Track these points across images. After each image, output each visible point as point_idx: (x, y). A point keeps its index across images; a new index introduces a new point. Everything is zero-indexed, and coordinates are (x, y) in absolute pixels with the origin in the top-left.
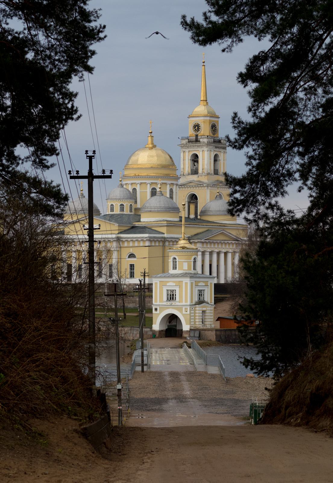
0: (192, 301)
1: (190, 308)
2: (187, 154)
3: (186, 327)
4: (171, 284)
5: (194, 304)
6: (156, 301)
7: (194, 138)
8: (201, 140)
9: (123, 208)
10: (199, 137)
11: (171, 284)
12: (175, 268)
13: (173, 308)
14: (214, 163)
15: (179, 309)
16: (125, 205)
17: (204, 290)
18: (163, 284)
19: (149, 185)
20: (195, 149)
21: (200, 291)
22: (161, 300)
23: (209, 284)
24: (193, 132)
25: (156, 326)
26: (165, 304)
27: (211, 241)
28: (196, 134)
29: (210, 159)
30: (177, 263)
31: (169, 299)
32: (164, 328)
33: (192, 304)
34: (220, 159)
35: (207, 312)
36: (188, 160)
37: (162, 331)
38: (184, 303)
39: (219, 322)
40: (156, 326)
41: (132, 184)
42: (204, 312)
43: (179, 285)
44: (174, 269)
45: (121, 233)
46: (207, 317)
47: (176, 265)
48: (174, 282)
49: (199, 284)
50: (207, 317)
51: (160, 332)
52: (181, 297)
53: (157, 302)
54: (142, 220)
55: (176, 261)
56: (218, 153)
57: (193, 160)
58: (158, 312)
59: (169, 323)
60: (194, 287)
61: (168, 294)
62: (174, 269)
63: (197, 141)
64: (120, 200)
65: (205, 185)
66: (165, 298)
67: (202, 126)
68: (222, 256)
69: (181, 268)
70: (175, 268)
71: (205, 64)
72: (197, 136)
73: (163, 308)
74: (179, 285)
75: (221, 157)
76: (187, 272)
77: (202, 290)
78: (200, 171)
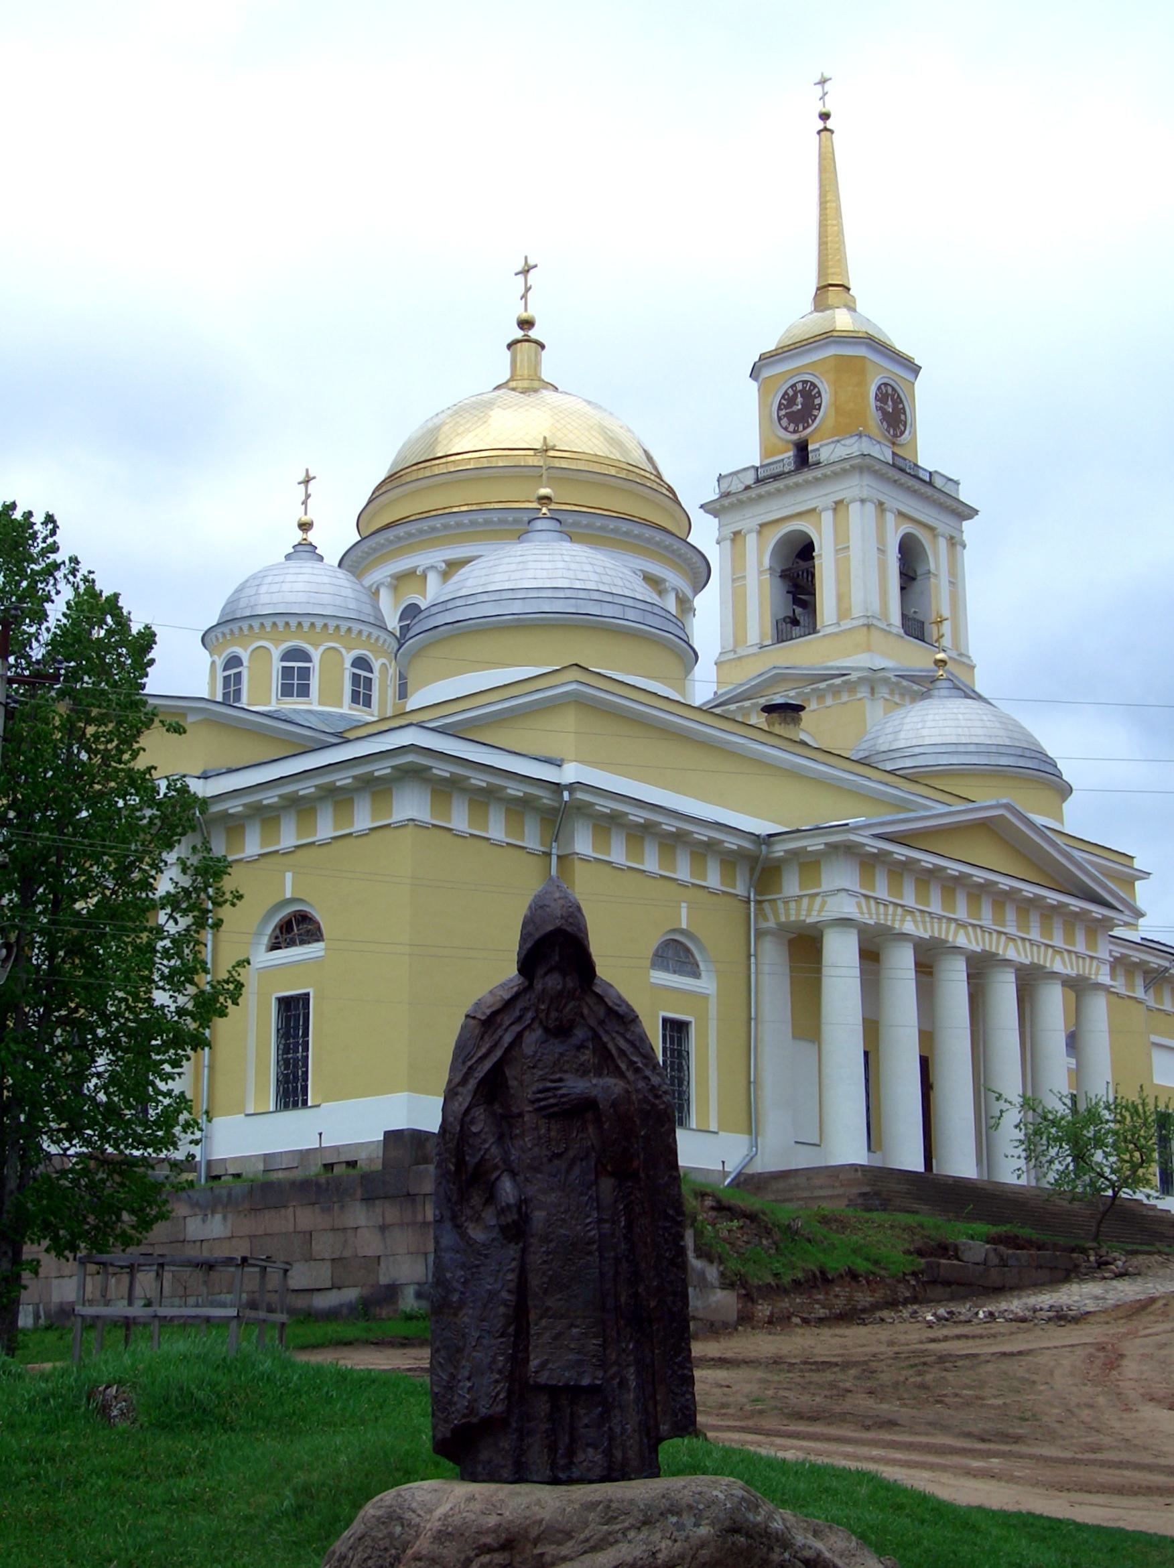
2: (751, 540)
9: (305, 673)
14: (902, 588)
16: (316, 654)
24: (782, 433)
27: (928, 860)
28: (795, 437)
29: (882, 551)
34: (932, 567)
36: (761, 573)
56: (923, 536)
57: (785, 575)
64: (280, 622)
65: (854, 676)
68: (1005, 991)
71: (830, 124)
72: (802, 449)
75: (937, 557)
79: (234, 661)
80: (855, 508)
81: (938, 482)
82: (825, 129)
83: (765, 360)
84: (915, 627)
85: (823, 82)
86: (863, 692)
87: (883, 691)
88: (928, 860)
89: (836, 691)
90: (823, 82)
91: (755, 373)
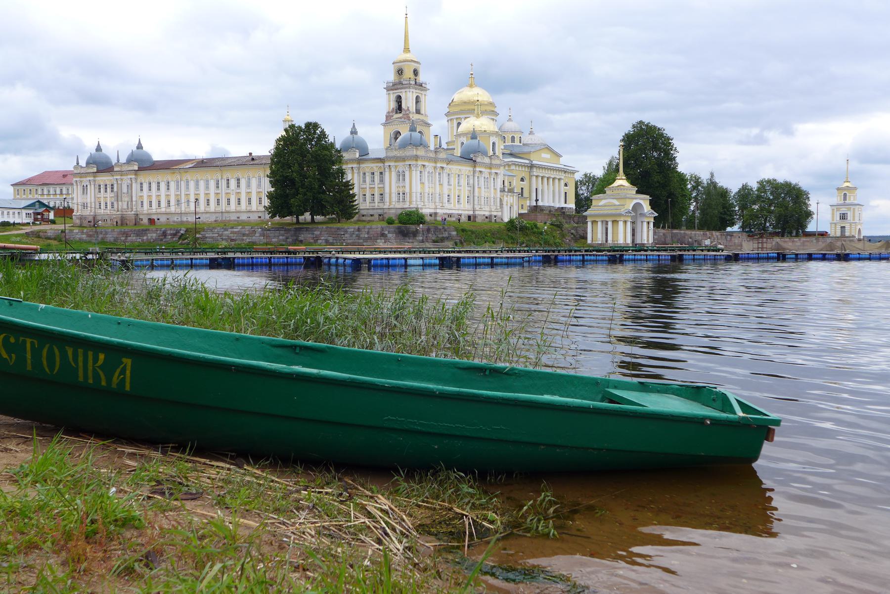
20: (419, 91)
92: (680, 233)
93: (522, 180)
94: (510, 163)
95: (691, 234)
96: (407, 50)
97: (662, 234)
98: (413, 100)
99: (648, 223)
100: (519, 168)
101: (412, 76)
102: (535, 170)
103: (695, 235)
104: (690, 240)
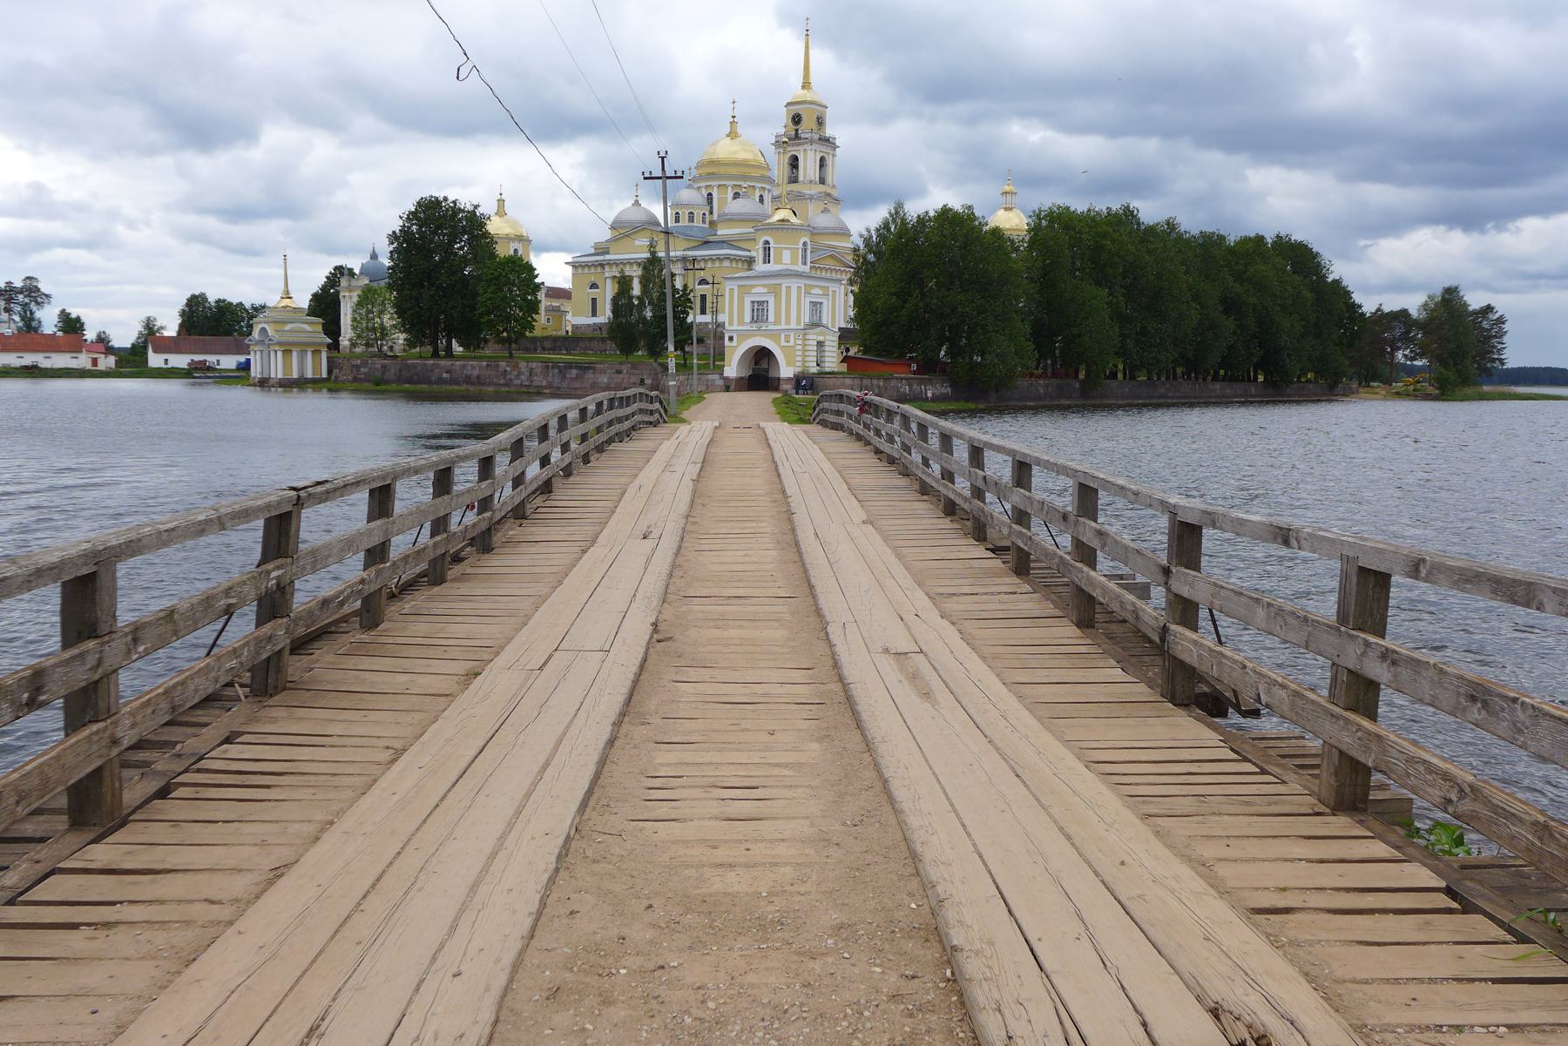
0: (798, 322)
1: (795, 334)
3: (786, 371)
4: (759, 291)
5: (802, 327)
6: (731, 323)
7: (794, 133)
8: (802, 136)
10: (799, 132)
11: (759, 291)
12: (767, 260)
13: (762, 335)
15: (775, 335)
17: (821, 303)
18: (744, 291)
19: (730, 188)
20: (794, 148)
21: (814, 304)
22: (741, 322)
23: (830, 293)
25: (732, 370)
26: (748, 328)
27: (817, 265)
29: (815, 162)
30: (771, 249)
31: (755, 318)
32: (746, 373)
33: (798, 327)
35: (827, 343)
37: (741, 378)
38: (783, 326)
39: (845, 365)
40: (732, 370)
41: (707, 187)
42: (820, 344)
43: (775, 291)
44: (765, 262)
45: (688, 249)
46: (826, 354)
47: (769, 254)
48: (764, 286)
49: (812, 292)
50: (826, 354)
51: (739, 380)
52: (777, 314)
53: (733, 325)
54: (718, 233)
55: (769, 248)
58: (735, 343)
59: (755, 365)
60: (803, 298)
61: (753, 310)
62: (765, 262)
63: (797, 136)
66: (748, 318)
67: (804, 117)
69: (779, 261)
70: (767, 260)
72: (797, 130)
73: (744, 335)
74: (775, 291)
75: (829, 161)
76: (791, 267)
77: (817, 303)
78: (801, 178)
79: (677, 213)
80: (809, 152)
81: (831, 140)
82: (807, 35)
83: (789, 104)
84: (822, 181)
85: (807, 19)
86: (809, 201)
87: (813, 201)
88: (817, 265)
89: (802, 200)
90: (807, 19)
91: (786, 106)
92: (426, 364)
93: (594, 286)
94: (707, 258)
95: (452, 365)
96: (806, 85)
97: (380, 366)
98: (815, 162)
99: (276, 351)
100: (737, 264)
101: (814, 125)
102: (607, 268)
103: (464, 366)
104: (444, 375)
